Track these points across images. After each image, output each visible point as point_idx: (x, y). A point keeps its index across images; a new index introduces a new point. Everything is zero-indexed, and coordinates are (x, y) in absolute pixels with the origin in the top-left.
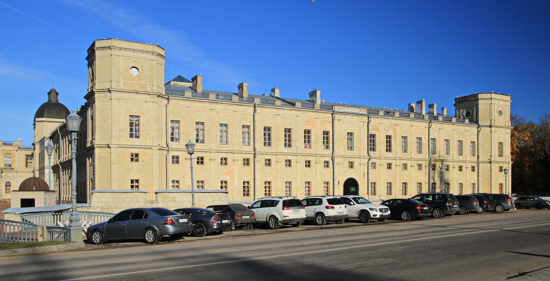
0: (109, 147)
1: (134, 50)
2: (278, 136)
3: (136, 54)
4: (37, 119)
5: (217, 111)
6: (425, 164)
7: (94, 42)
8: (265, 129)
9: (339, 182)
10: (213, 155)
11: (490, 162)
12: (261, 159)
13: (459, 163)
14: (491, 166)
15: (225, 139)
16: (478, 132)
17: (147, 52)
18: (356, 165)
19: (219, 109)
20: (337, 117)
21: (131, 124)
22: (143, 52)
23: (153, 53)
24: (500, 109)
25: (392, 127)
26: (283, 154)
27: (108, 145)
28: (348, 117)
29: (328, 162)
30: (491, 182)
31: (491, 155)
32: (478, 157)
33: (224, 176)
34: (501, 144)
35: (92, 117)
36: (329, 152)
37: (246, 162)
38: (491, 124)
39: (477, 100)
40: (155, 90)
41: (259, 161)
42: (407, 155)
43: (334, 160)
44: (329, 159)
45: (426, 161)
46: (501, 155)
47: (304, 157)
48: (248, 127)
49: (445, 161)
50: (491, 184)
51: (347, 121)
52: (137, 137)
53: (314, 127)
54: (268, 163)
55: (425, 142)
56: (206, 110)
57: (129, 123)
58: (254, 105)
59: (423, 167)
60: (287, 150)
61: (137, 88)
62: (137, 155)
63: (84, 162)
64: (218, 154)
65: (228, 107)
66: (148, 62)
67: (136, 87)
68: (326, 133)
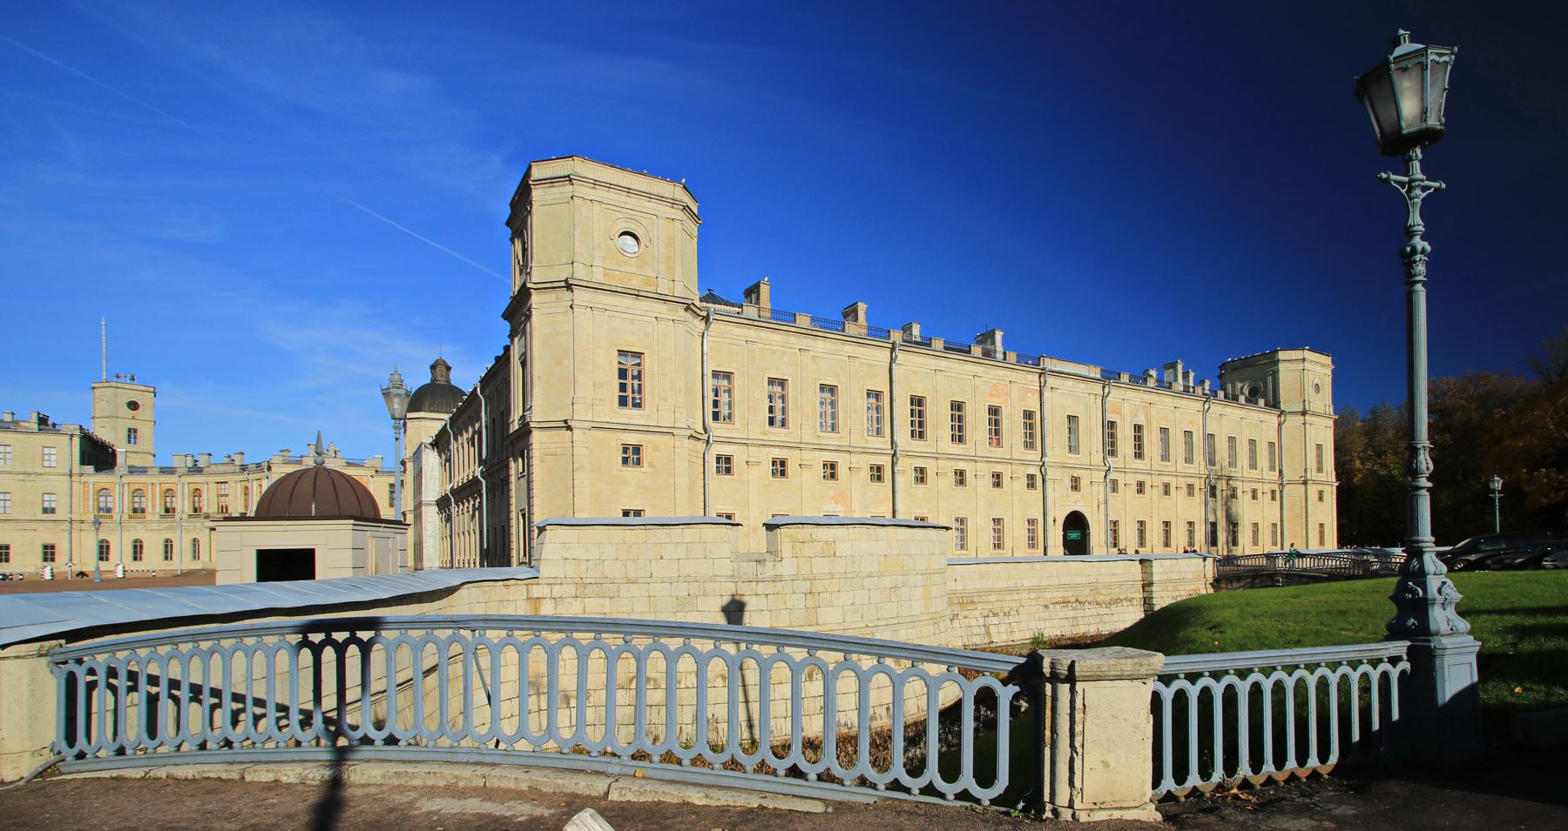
0: (569, 428)
1: (629, 191)
2: (938, 418)
3: (633, 201)
4: (409, 415)
5: (813, 354)
6: (1199, 484)
7: (530, 167)
9: (1055, 521)
10: (807, 456)
11: (1305, 483)
12: (906, 467)
14: (1306, 490)
16: (1279, 425)
17: (660, 198)
18: (1084, 483)
19: (819, 350)
20: (1051, 381)
21: (623, 373)
22: (649, 196)
23: (674, 203)
24: (1316, 381)
25: (1143, 407)
27: (565, 421)
28: (1069, 383)
29: (1031, 477)
30: (1307, 521)
31: (1306, 469)
32: (1281, 472)
34: (1319, 447)
35: (523, 358)
36: (1034, 455)
37: (877, 473)
38: (1304, 408)
40: (679, 291)
41: (903, 472)
42: (1168, 466)
44: (1034, 470)
46: (1320, 470)
47: (989, 465)
48: (877, 395)
50: (1307, 525)
51: (1067, 392)
52: (637, 405)
53: (1006, 401)
54: (921, 476)
55: (1198, 439)
56: (789, 350)
57: (617, 370)
58: (890, 346)
60: (957, 449)
61: (635, 283)
62: (637, 449)
63: (502, 480)
64: (818, 453)
65: (836, 346)
66: (662, 222)
67: (634, 282)
68: (1028, 415)
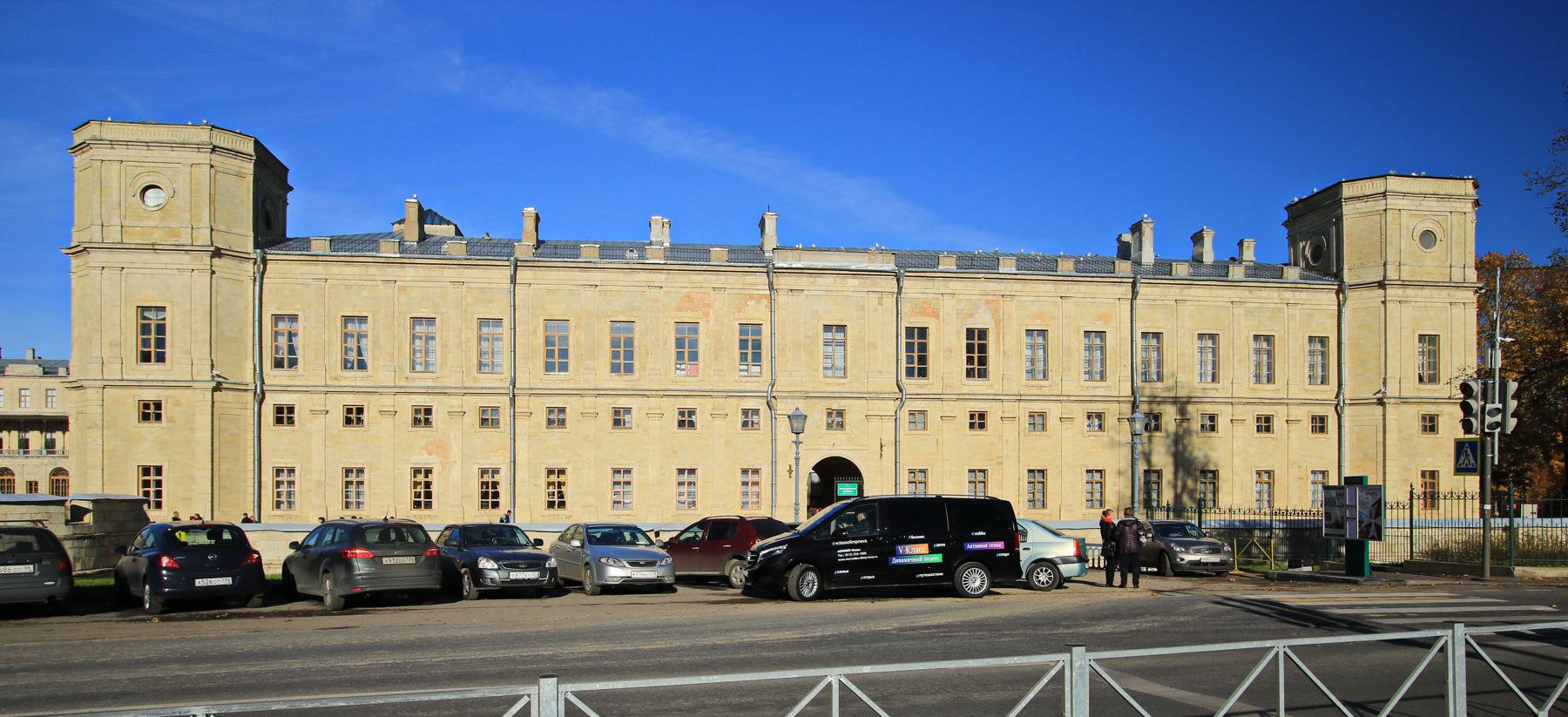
1: (147, 144)
3: (155, 154)
5: (402, 284)
8: (970, 333)
11: (1381, 402)
13: (1255, 407)
14: (1384, 415)
15: (1040, 366)
19: (408, 279)
20: (782, 282)
22: (172, 145)
26: (599, 393)
28: (827, 281)
30: (1384, 467)
31: (1385, 379)
33: (422, 454)
39: (1338, 204)
43: (1342, 412)
45: (1287, 404)
47: (673, 399)
49: (1193, 400)
53: (706, 314)
54: (556, 418)
55: (1117, 342)
56: (371, 283)
59: (1110, 421)
60: (619, 381)
61: (157, 237)
65: (435, 272)
67: (156, 236)
